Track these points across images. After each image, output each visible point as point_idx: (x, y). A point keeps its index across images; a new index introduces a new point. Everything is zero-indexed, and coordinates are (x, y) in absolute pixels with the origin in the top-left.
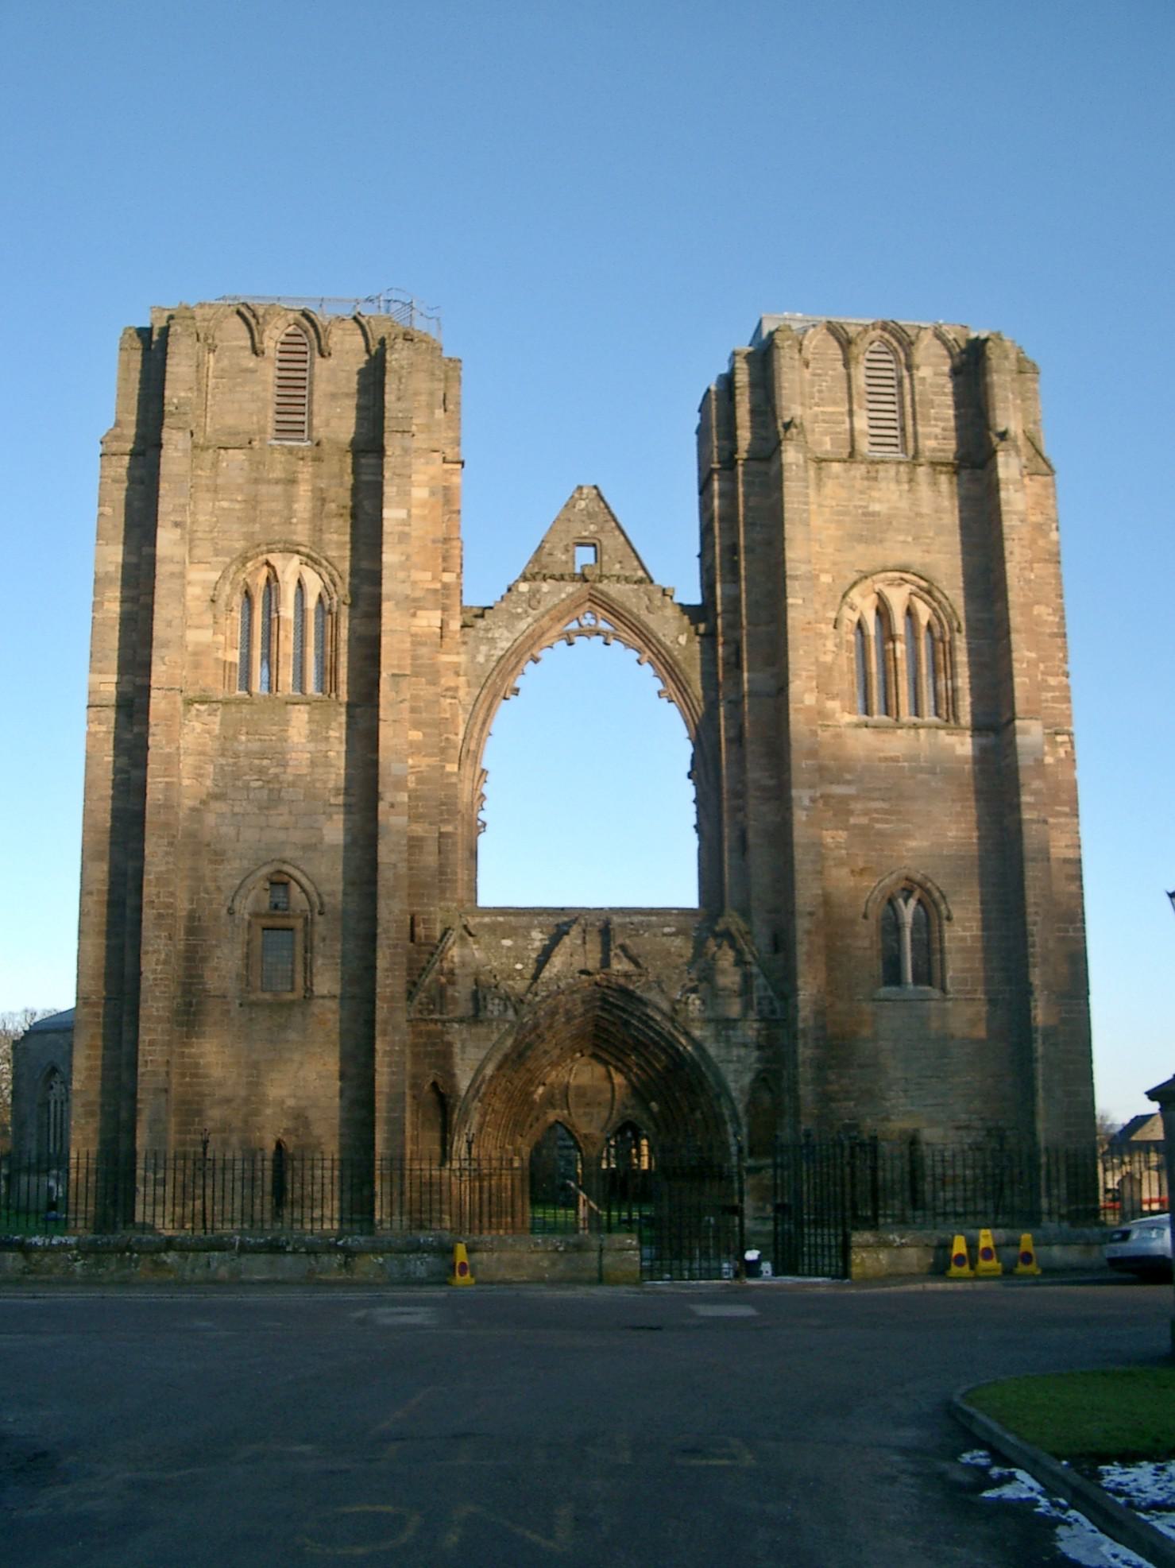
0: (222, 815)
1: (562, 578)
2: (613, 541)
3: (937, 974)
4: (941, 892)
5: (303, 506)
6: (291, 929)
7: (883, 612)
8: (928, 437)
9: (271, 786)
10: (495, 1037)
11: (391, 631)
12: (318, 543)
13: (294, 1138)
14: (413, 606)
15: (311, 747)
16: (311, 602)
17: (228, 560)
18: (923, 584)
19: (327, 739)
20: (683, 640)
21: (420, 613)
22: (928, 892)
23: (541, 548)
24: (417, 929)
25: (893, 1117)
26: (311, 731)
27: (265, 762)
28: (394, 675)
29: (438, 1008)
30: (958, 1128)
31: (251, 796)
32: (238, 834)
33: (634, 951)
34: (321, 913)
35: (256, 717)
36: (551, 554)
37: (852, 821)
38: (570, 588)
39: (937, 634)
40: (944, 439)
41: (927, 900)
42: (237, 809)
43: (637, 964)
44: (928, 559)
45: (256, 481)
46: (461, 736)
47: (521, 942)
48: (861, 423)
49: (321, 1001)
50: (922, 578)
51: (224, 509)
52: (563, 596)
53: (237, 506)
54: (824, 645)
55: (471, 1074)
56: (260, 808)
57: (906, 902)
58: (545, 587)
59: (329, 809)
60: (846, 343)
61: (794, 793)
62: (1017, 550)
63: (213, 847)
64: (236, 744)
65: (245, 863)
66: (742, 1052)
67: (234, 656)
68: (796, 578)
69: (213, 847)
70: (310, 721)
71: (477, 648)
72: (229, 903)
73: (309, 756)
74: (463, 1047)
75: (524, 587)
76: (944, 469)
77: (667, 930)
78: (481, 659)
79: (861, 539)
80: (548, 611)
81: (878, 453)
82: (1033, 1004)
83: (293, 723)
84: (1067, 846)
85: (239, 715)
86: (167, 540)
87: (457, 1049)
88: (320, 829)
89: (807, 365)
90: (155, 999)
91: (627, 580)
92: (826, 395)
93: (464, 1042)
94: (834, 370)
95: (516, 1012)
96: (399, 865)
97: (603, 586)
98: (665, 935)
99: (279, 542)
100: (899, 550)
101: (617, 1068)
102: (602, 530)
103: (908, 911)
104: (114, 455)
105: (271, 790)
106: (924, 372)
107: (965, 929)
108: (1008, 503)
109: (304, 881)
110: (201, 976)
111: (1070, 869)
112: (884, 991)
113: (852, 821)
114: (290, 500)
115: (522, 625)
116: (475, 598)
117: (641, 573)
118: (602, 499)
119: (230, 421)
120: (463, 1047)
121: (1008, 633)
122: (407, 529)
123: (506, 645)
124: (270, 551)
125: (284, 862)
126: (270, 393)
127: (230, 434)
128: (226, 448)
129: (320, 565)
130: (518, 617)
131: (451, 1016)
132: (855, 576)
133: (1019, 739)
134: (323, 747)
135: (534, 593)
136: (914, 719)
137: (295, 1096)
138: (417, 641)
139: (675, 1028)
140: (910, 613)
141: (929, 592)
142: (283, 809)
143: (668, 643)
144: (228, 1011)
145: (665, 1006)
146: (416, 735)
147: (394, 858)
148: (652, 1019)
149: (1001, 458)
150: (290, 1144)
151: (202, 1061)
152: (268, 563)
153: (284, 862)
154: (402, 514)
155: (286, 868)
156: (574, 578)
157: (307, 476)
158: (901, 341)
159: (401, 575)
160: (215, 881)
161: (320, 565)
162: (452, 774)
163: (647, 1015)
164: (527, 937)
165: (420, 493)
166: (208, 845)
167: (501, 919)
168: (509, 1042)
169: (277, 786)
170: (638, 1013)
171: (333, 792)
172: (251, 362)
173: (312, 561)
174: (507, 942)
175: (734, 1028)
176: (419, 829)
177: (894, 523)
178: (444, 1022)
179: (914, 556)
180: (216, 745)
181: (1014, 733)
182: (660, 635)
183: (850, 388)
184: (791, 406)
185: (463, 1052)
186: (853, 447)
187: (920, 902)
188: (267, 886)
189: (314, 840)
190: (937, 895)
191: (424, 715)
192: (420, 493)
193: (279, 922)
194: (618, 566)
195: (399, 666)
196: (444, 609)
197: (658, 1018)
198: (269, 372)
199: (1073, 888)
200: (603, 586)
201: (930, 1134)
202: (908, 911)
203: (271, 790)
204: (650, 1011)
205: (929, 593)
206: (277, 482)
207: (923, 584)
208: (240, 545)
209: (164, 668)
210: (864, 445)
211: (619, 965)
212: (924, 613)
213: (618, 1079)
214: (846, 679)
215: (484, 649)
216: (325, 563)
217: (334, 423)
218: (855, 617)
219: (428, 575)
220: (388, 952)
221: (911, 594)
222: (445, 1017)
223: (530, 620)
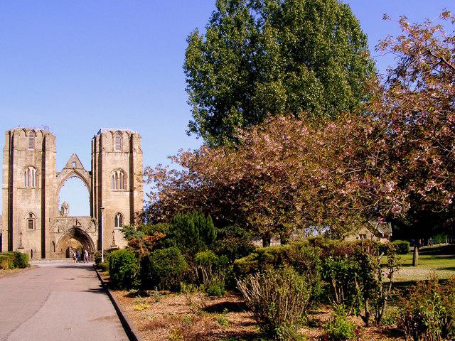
2: (78, 162)
7: (116, 174)
48: (115, 145)
60: (113, 134)
67: (24, 181)
81: (117, 151)
86: (14, 166)
100: (119, 166)
103: (118, 217)
116: (58, 171)
126: (28, 142)
158: (120, 133)
165: (51, 158)
173: (34, 168)
184: (104, 145)
192: (51, 158)
198: (28, 138)
202: (118, 217)
210: (115, 149)
211: (78, 225)
212: (122, 174)
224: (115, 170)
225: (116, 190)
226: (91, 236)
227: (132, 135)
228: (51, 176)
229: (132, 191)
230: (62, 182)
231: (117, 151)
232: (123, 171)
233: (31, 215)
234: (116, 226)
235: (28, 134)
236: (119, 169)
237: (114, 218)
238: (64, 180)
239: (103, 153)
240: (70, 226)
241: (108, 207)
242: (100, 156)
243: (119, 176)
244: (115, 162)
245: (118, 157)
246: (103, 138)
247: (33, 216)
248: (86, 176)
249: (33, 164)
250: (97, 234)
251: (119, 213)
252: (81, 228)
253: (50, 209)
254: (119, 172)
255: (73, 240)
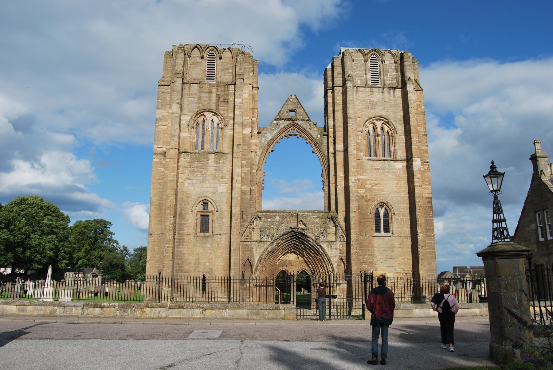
0: (190, 184)
1: (285, 120)
2: (299, 110)
3: (391, 229)
4: (392, 206)
5: (214, 99)
6: (208, 216)
8: (387, 80)
9: (204, 176)
10: (265, 246)
11: (237, 132)
12: (217, 109)
13: (208, 274)
14: (243, 126)
15: (215, 165)
16: (215, 125)
17: (193, 114)
18: (386, 121)
19: (219, 163)
20: (319, 136)
21: (245, 128)
22: (388, 206)
23: (280, 112)
24: (243, 216)
25: (378, 270)
26: (215, 161)
27: (202, 169)
28: (238, 145)
29: (249, 238)
30: (397, 273)
31: (198, 178)
32: (194, 189)
33: (305, 222)
34: (217, 211)
35: (200, 157)
36: (283, 114)
37: (366, 186)
38: (288, 122)
39: (390, 134)
40: (392, 81)
41: (387, 208)
42: (194, 182)
43: (306, 226)
44: (388, 113)
45: (201, 92)
46: (257, 163)
47: (273, 220)
48: (369, 76)
49: (216, 236)
50: (386, 119)
51: (192, 100)
52: (286, 124)
53: (196, 99)
54: (359, 137)
55: (259, 257)
56: (200, 182)
57: (381, 208)
58: (281, 122)
59: (220, 182)
60: (365, 55)
61: (350, 178)
62: (413, 111)
63: (187, 193)
64: (194, 164)
65: (196, 197)
66: (335, 251)
67: (194, 141)
68: (350, 118)
69: (187, 193)
70: (215, 158)
71: (262, 138)
72: (191, 208)
73: (214, 167)
74: (256, 250)
75: (275, 122)
76: (392, 89)
77: (314, 217)
78: (263, 142)
79: (368, 108)
80: (282, 129)
82: (418, 238)
83: (210, 158)
84: (427, 194)
85: (195, 156)
87: (254, 250)
88: (217, 188)
89: (353, 61)
90: (169, 235)
91: (304, 120)
92: (359, 69)
93: (256, 247)
94: (361, 62)
95: (272, 239)
96: (238, 197)
97: (297, 122)
98: (313, 218)
99: (207, 109)
100: (379, 112)
101: (300, 256)
102: (297, 107)
103: (382, 212)
104: (162, 86)
105: (203, 177)
106: (386, 62)
107: (399, 216)
108: (410, 98)
109: (212, 202)
110: (183, 229)
111: (429, 200)
112: (376, 234)
113: (366, 186)
114: (210, 98)
115: (275, 132)
117: (308, 119)
118: (297, 98)
119: (194, 76)
120: (256, 250)
121: (410, 133)
122: (242, 105)
123: (270, 138)
124: (204, 112)
125: (207, 197)
127: (194, 80)
128: (192, 84)
129: (218, 115)
130: (273, 130)
131: (253, 240)
132: (367, 119)
133: (414, 163)
134: (218, 165)
135: (278, 124)
136: (384, 158)
137: (209, 263)
138: (244, 136)
139: (316, 244)
140: (382, 129)
141: (388, 122)
142: (207, 182)
143: (315, 137)
144: (191, 238)
145: (313, 238)
146: (244, 162)
147: (237, 195)
148: (310, 241)
149: (408, 85)
150: (207, 276)
151: (183, 253)
152: (203, 115)
153: (207, 197)
154: (240, 100)
155: (207, 199)
156: (289, 119)
157: (215, 91)
159: (240, 117)
160: (187, 202)
161: (218, 115)
162: (254, 173)
163: (308, 240)
164: (275, 218)
165: (246, 96)
166: (186, 192)
167: (268, 213)
168: (270, 247)
169: (205, 176)
170: (306, 240)
171: (221, 178)
172: (200, 60)
173: (216, 114)
174: (269, 220)
175: (333, 244)
176: (245, 188)
177: (378, 104)
178: (251, 242)
179: (384, 113)
180: (188, 164)
181: (412, 161)
182: (313, 135)
183: (365, 67)
184: (348, 71)
185: (256, 250)
186: (366, 83)
187: (385, 209)
188: (202, 204)
189: (215, 191)
190: (390, 207)
191: (246, 156)
193: (205, 214)
194: (301, 117)
195: (239, 142)
196: (252, 128)
197: (311, 241)
198: (205, 63)
199: (429, 205)
200: (297, 122)
201: (389, 275)
202: (382, 212)
203: (203, 177)
204: (309, 239)
205: (388, 123)
206: (207, 92)
207: (386, 121)
208: (196, 110)
209: (173, 143)
210: (369, 83)
212: (386, 128)
213: (301, 259)
214: (364, 148)
215: (264, 139)
216: (219, 115)
217: (222, 77)
218: (367, 130)
219: (248, 118)
220: (235, 222)
221: (382, 123)
222: (251, 240)
223: (276, 131)
224: (372, 119)
225: (373, 158)
226: (327, 250)
227: (402, 56)
228: (248, 130)
229: (409, 160)
230: (269, 145)
231: (374, 85)
232: (387, 122)
233: (205, 203)
234: (378, 230)
235: (206, 57)
236: (380, 118)
237: (374, 212)
238: (273, 140)
239: (349, 84)
240: (284, 228)
241: (362, 191)
242: (344, 93)
243: (379, 132)
244: (372, 105)
245: (377, 95)
246: (347, 59)
247: (210, 207)
248: (315, 133)
249: (213, 107)
250: (341, 245)
251: (382, 205)
252: (306, 232)
253: (243, 192)
254: (379, 124)
255: (292, 257)
